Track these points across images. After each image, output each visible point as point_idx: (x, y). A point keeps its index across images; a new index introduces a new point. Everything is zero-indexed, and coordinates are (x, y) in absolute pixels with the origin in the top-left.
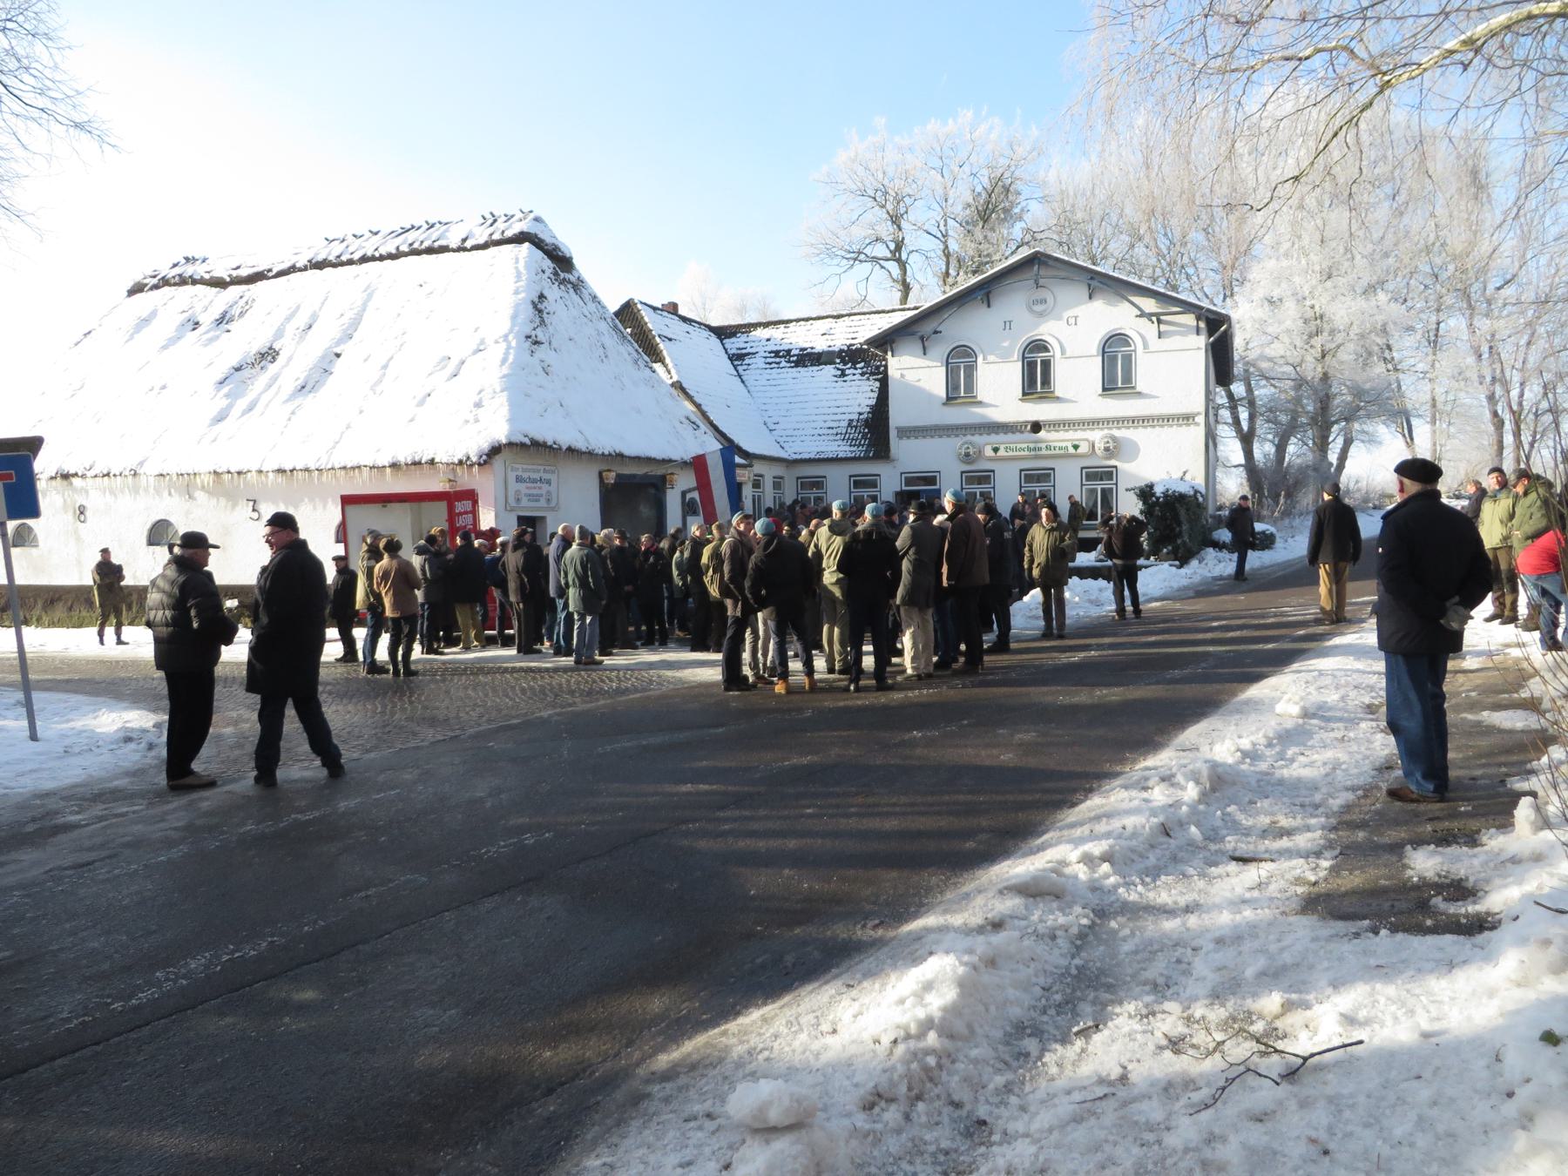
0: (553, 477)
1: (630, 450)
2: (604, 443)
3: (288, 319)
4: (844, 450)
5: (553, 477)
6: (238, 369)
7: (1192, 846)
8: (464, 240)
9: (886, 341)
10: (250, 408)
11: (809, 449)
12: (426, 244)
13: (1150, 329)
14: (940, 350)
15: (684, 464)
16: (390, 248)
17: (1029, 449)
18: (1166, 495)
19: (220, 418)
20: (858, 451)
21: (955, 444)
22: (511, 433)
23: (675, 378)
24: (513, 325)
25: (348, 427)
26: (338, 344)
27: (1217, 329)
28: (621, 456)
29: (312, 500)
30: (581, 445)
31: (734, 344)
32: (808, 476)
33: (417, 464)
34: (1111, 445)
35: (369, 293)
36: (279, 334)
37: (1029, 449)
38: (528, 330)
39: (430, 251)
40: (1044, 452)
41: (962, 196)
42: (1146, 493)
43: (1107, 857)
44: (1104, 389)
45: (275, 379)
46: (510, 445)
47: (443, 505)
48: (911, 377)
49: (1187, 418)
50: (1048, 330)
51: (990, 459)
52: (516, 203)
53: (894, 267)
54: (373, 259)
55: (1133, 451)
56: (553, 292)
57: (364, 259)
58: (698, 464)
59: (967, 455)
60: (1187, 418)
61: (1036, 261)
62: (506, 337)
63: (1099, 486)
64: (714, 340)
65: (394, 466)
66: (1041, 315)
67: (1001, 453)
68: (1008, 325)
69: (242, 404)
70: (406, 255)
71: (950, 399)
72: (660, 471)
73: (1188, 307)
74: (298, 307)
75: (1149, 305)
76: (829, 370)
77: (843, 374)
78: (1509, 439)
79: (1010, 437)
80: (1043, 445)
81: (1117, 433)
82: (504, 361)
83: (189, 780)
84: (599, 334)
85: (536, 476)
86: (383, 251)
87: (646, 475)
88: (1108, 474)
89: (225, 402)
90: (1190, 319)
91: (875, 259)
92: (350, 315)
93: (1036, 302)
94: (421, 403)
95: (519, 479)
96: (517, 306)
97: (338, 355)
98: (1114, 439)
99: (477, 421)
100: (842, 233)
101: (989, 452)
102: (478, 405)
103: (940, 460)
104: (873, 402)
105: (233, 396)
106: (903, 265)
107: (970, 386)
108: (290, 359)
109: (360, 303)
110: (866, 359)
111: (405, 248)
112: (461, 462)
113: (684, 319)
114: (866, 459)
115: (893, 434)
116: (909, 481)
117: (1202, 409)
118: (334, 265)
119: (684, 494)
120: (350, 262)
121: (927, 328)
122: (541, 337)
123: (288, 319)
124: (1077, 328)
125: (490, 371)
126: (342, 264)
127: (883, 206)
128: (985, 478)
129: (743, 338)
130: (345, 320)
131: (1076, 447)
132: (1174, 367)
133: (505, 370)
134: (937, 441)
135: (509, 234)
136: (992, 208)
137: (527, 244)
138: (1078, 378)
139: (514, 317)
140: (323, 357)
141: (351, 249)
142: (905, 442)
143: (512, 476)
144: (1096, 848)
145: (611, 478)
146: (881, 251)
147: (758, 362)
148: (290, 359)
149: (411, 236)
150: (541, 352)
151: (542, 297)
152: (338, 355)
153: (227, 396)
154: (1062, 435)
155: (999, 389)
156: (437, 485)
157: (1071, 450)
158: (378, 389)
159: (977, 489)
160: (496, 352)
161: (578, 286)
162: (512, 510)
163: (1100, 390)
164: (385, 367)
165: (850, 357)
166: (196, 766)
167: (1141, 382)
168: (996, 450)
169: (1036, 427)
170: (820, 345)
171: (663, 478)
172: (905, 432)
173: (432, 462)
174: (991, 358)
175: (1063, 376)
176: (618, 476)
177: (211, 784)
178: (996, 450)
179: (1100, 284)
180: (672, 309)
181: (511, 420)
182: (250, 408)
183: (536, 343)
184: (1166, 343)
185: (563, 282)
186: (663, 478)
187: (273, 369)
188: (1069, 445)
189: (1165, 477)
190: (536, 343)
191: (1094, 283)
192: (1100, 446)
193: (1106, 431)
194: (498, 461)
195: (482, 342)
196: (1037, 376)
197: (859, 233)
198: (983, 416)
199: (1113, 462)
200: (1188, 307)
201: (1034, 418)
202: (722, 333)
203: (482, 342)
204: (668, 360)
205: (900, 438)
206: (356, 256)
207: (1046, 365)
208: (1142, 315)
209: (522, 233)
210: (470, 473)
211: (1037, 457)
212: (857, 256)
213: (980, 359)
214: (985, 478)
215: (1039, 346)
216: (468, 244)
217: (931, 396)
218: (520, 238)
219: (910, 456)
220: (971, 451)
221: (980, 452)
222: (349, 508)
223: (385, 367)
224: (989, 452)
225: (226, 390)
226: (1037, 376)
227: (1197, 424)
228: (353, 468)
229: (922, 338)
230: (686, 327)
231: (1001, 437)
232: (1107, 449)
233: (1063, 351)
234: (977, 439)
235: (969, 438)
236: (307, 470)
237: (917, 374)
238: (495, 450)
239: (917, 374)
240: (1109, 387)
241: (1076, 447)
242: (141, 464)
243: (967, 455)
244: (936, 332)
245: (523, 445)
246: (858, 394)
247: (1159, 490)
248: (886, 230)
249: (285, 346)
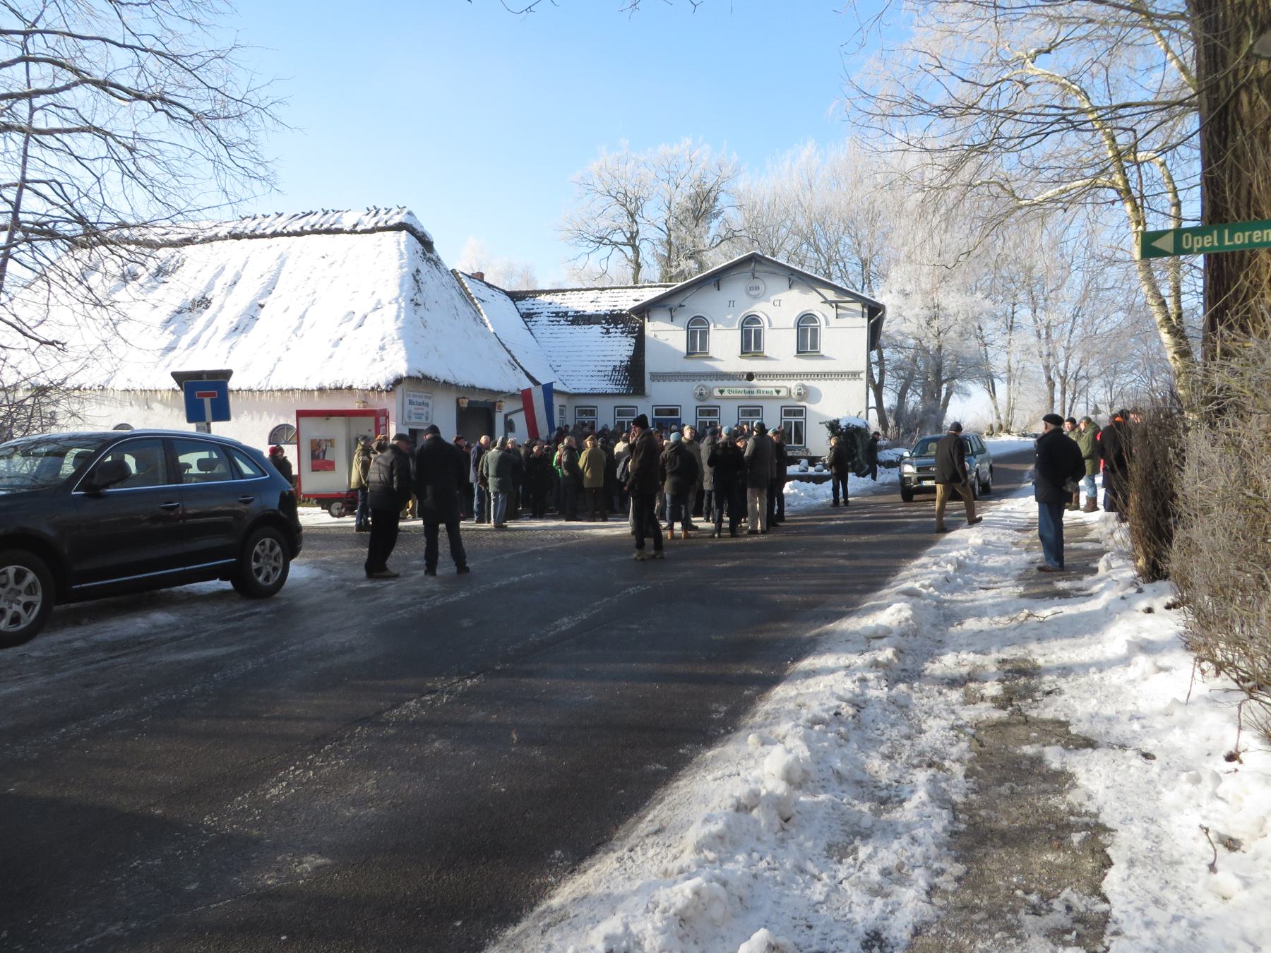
0: (430, 402)
1: (479, 385)
2: (464, 379)
3: (217, 276)
4: (610, 387)
5: (430, 402)
6: (179, 312)
7: (959, 585)
8: (355, 226)
9: (644, 310)
10: (194, 342)
11: (585, 386)
12: (325, 226)
13: (831, 312)
14: (684, 319)
15: (512, 396)
16: (296, 226)
18: (847, 427)
19: (170, 349)
20: (622, 389)
21: (693, 386)
22: (409, 369)
23: (492, 330)
24: (401, 291)
25: (279, 360)
26: (261, 297)
27: (874, 312)
28: (474, 388)
29: (250, 412)
30: (451, 379)
31: (525, 305)
32: (584, 403)
33: (338, 389)
35: (282, 260)
36: (210, 287)
38: (412, 296)
39: (328, 231)
41: (681, 198)
42: (834, 426)
43: (930, 586)
44: (798, 352)
45: (211, 321)
46: (409, 378)
47: (372, 420)
48: (661, 337)
49: (855, 375)
50: (759, 309)
51: (717, 398)
52: (397, 200)
53: (629, 250)
54: (282, 234)
56: (424, 267)
57: (275, 234)
58: (526, 396)
59: (701, 394)
60: (855, 375)
61: (752, 259)
62: (397, 299)
63: (793, 420)
64: (509, 300)
65: (321, 390)
66: (756, 298)
69: (186, 340)
70: (309, 233)
71: (690, 353)
72: (492, 399)
73: (857, 298)
74: (223, 268)
75: (830, 295)
76: (597, 329)
77: (608, 332)
78: (1058, 396)
79: (731, 383)
81: (806, 383)
82: (398, 317)
83: (386, 573)
84: (453, 299)
85: (420, 400)
86: (290, 229)
87: (485, 402)
88: (799, 412)
89: (173, 337)
90: (857, 307)
91: (616, 244)
92: (267, 276)
94: (336, 345)
95: (411, 403)
96: (402, 278)
97: (262, 306)
98: (804, 387)
99: (382, 360)
100: (591, 222)
101: (716, 393)
102: (382, 348)
103: (681, 396)
104: (631, 353)
105: (178, 334)
106: (636, 249)
108: (221, 307)
109: (275, 267)
110: (630, 323)
111: (307, 228)
112: (373, 389)
113: (489, 286)
114: (627, 394)
115: (647, 377)
116: (658, 412)
117: (864, 369)
118: (250, 237)
119: (506, 416)
120: (263, 236)
121: (675, 302)
122: (420, 299)
123: (217, 276)
124: (781, 308)
125: (387, 322)
126: (257, 237)
127: (624, 205)
128: (713, 411)
129: (531, 301)
130: (265, 279)
131: (778, 392)
132: (845, 339)
133: (399, 324)
135: (391, 223)
136: (701, 208)
137: (404, 232)
138: (780, 344)
139: (401, 285)
140: (250, 307)
141: (263, 226)
143: (407, 402)
144: (927, 583)
145: (465, 403)
146: (619, 237)
147: (543, 319)
148: (221, 307)
149: (312, 220)
150: (421, 310)
151: (418, 271)
152: (262, 306)
153: (173, 333)
154: (768, 383)
155: (724, 347)
156: (355, 405)
157: (775, 394)
158: (299, 333)
159: (708, 419)
160: (390, 311)
161: (437, 263)
162: (406, 424)
164: (302, 317)
165: (613, 319)
166: (390, 563)
167: (824, 348)
168: (722, 392)
169: (750, 376)
170: (590, 309)
171: (494, 404)
172: (657, 377)
173: (350, 388)
174: (719, 326)
176: (470, 402)
177: (396, 576)
178: (722, 392)
179: (797, 278)
180: (479, 277)
181: (408, 361)
182: (194, 342)
183: (417, 304)
184: (841, 322)
185: (429, 260)
186: (494, 404)
187: (208, 314)
189: (845, 415)
190: (417, 304)
191: (793, 278)
192: (794, 392)
194: (399, 389)
195: (379, 302)
196: (751, 343)
197: (604, 224)
199: (803, 403)
200: (857, 298)
202: (515, 296)
203: (379, 302)
204: (485, 317)
205: (653, 380)
206: (269, 231)
208: (826, 301)
209: (401, 223)
210: (380, 397)
211: (750, 398)
212: (601, 241)
214: (713, 411)
215: (752, 319)
216: (359, 228)
217: (675, 352)
218: (399, 227)
219: (660, 394)
221: (710, 393)
222: (302, 420)
223: (302, 317)
224: (716, 393)
225: (172, 328)
226: (751, 343)
228: (288, 390)
229: (671, 310)
230: (490, 291)
231: (726, 383)
232: (799, 394)
233: (770, 324)
235: (703, 382)
236: (250, 390)
237: (666, 335)
238: (398, 381)
240: (801, 352)
241: (778, 392)
242: (108, 381)
243: (701, 394)
245: (418, 378)
246: (620, 347)
247: (843, 424)
248: (625, 222)
249: (216, 295)
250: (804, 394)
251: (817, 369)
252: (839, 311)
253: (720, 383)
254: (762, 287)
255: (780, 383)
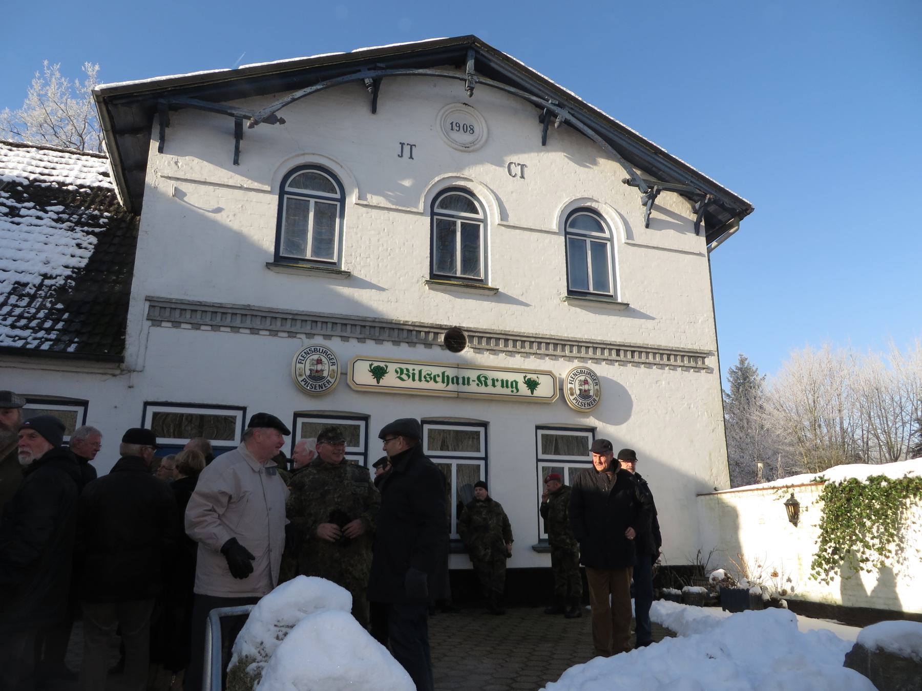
17: (446, 379)
34: (591, 387)
37: (446, 379)
40: (473, 387)
48: (196, 198)
51: (364, 392)
55: (622, 408)
59: (316, 376)
60: (693, 359)
61: (461, 59)
66: (466, 148)
67: (390, 379)
68: (407, 149)
71: (283, 261)
79: (404, 351)
80: (473, 375)
81: (602, 370)
93: (455, 126)
101: (363, 375)
107: (325, 241)
114: (54, 356)
115: (137, 311)
134: (244, 339)
138: (524, 266)
142: (165, 333)
155: (382, 253)
163: (565, 293)
168: (378, 373)
169: (455, 339)
172: (166, 311)
174: (374, 200)
175: (499, 255)
178: (378, 373)
188: (520, 378)
193: (576, 363)
196: (455, 251)
198: (356, 304)
201: (454, 322)
205: (155, 321)
207: (472, 233)
213: (352, 199)
217: (239, 242)
219: (170, 367)
220: (326, 369)
224: (363, 375)
226: (455, 251)
227: (709, 370)
232: (584, 395)
233: (504, 215)
234: (335, 345)
235: (319, 341)
239: (211, 196)
240: (576, 293)
243: (316, 376)
244: (272, 119)
250: (592, 397)
251: (616, 338)
252: (655, 214)
253: (371, 348)
254: (480, 128)
255: (532, 363)
